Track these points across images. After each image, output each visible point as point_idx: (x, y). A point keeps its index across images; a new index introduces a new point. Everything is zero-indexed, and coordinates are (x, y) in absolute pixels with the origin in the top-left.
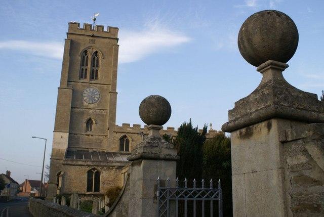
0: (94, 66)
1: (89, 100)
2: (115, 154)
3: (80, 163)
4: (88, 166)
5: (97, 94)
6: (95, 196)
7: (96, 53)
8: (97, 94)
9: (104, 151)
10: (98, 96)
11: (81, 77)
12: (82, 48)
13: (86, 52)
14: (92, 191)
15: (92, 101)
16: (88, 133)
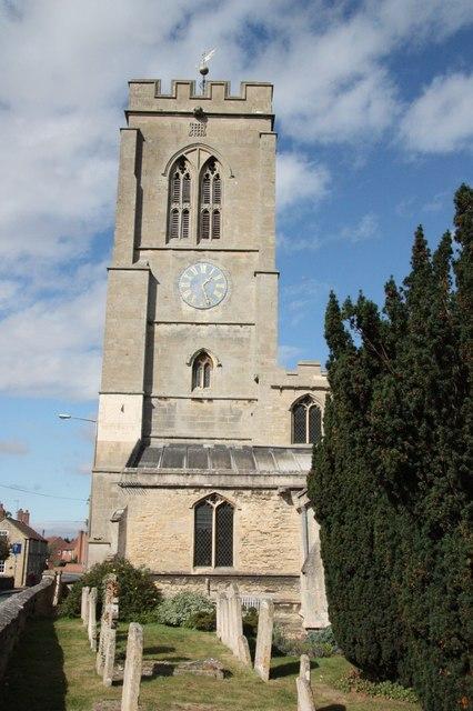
0: (207, 202)
2: (280, 452)
3: (171, 480)
5: (220, 282)
7: (211, 162)
8: (220, 282)
10: (223, 286)
12: (171, 152)
13: (181, 162)
14: (210, 564)
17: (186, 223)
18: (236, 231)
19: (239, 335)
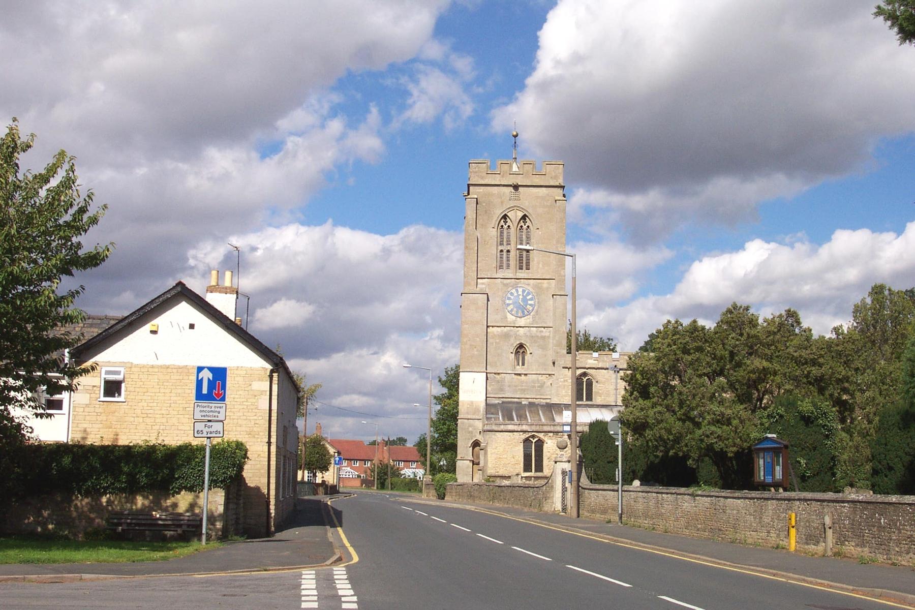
1: (517, 312)
3: (511, 427)
4: (524, 432)
6: (537, 478)
9: (548, 401)
11: (501, 267)
12: (498, 213)
15: (523, 312)
16: (519, 369)
17: (508, 260)
18: (541, 266)
19: (543, 334)
